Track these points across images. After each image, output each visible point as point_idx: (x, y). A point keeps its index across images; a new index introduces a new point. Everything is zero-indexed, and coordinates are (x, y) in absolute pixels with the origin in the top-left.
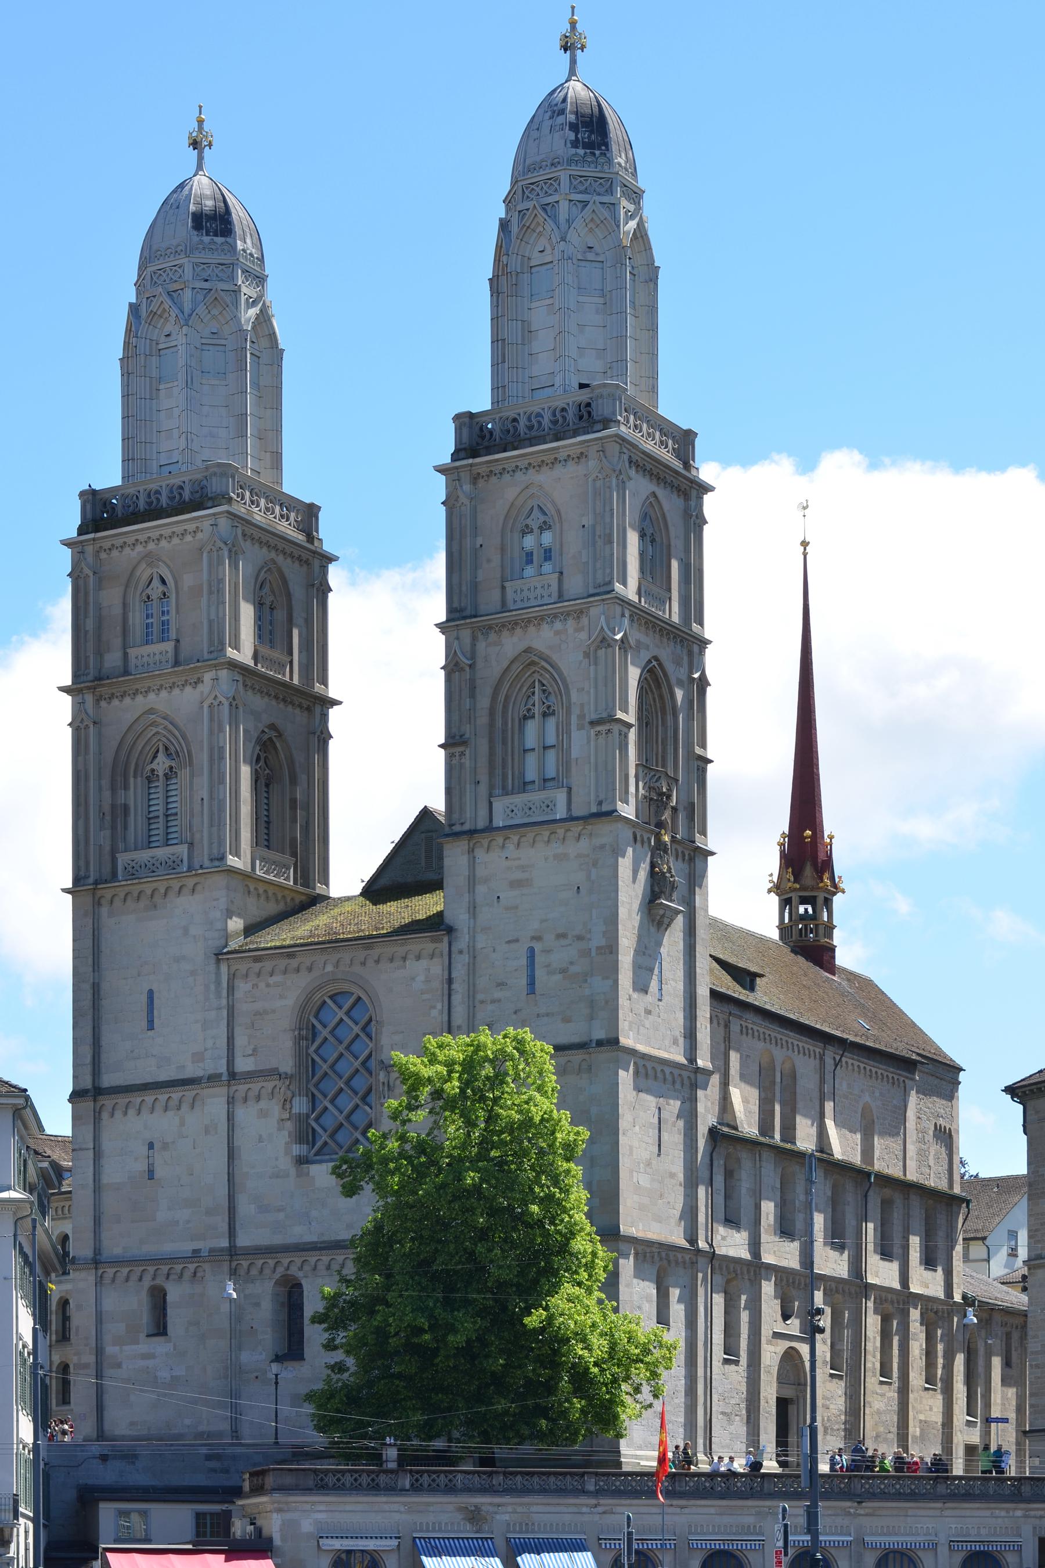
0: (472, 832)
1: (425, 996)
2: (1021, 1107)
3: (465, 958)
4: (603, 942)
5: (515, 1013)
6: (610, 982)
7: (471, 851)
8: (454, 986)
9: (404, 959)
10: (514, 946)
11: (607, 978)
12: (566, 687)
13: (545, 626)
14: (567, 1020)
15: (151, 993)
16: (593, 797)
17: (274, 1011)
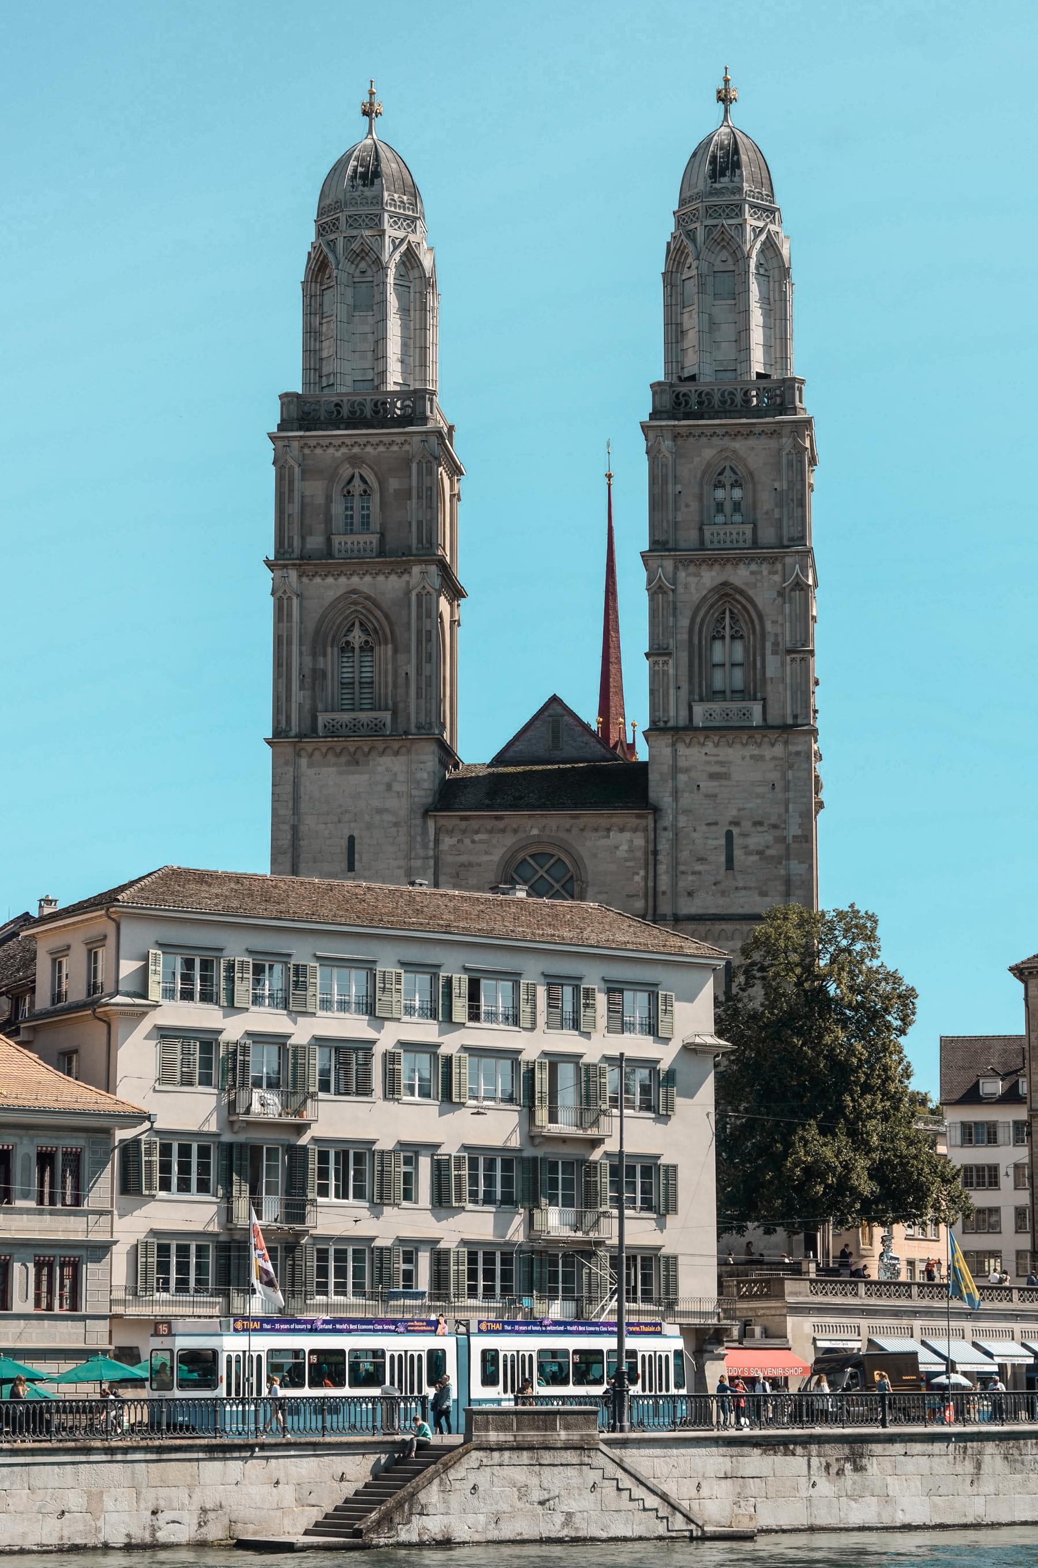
0: (676, 729)
1: (629, 864)
2: (1021, 986)
3: (669, 835)
4: (799, 832)
5: (715, 884)
6: (806, 866)
7: (673, 745)
8: (659, 857)
9: (609, 830)
10: (714, 828)
11: (803, 862)
12: (760, 617)
13: (741, 566)
14: (763, 894)
15: (351, 839)
16: (789, 711)
17: (479, 865)
